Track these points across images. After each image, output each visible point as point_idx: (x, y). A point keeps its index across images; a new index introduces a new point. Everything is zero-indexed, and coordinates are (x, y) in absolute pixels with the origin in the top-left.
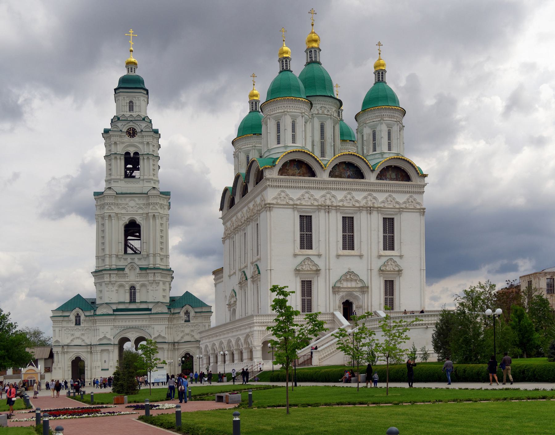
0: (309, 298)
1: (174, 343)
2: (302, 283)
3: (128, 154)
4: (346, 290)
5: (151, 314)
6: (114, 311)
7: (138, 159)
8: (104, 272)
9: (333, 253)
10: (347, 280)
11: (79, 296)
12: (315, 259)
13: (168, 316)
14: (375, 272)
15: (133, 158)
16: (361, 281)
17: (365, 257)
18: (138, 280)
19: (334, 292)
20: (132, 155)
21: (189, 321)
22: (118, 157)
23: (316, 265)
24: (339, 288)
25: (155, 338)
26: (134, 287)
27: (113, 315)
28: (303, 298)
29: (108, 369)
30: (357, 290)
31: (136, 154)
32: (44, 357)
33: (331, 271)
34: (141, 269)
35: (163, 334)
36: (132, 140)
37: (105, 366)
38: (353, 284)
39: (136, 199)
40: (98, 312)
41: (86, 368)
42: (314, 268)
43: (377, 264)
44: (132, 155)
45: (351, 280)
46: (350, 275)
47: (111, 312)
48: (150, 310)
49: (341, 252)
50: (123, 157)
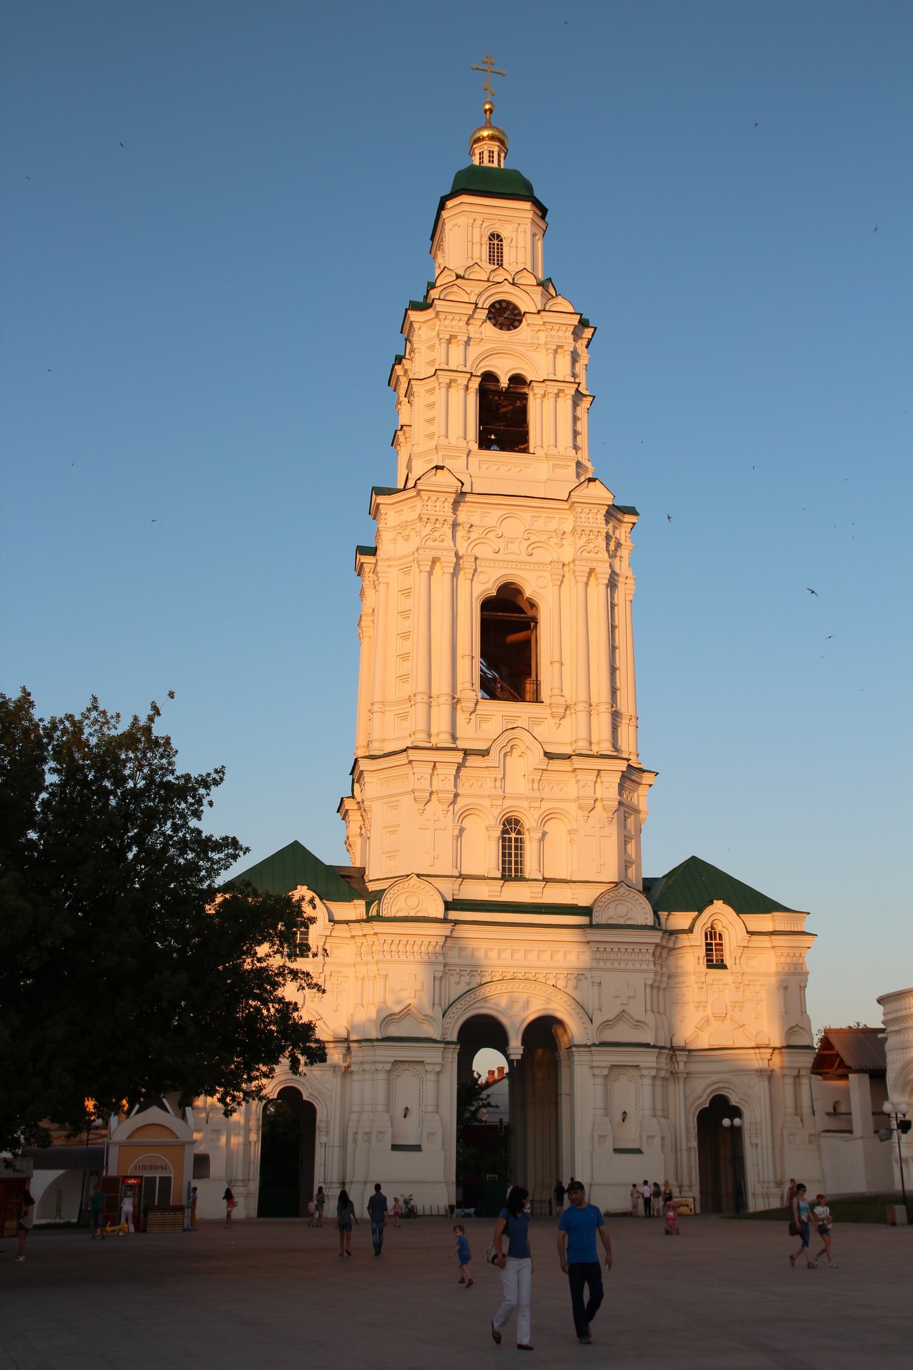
1: (673, 1049)
3: (489, 378)
5: (591, 926)
6: (449, 906)
7: (524, 397)
8: (413, 755)
11: (296, 847)
13: (656, 937)
15: (508, 393)
18: (537, 794)
20: (504, 383)
21: (722, 966)
22: (462, 380)
25: (607, 1024)
26: (517, 822)
27: (445, 920)
29: (417, 1148)
31: (517, 380)
32: (772, 1045)
34: (549, 756)
35: (637, 1009)
36: (505, 335)
37: (409, 1133)
39: (527, 515)
40: (390, 906)
41: (320, 1138)
44: (504, 383)
47: (438, 911)
48: (586, 911)
50: (475, 384)
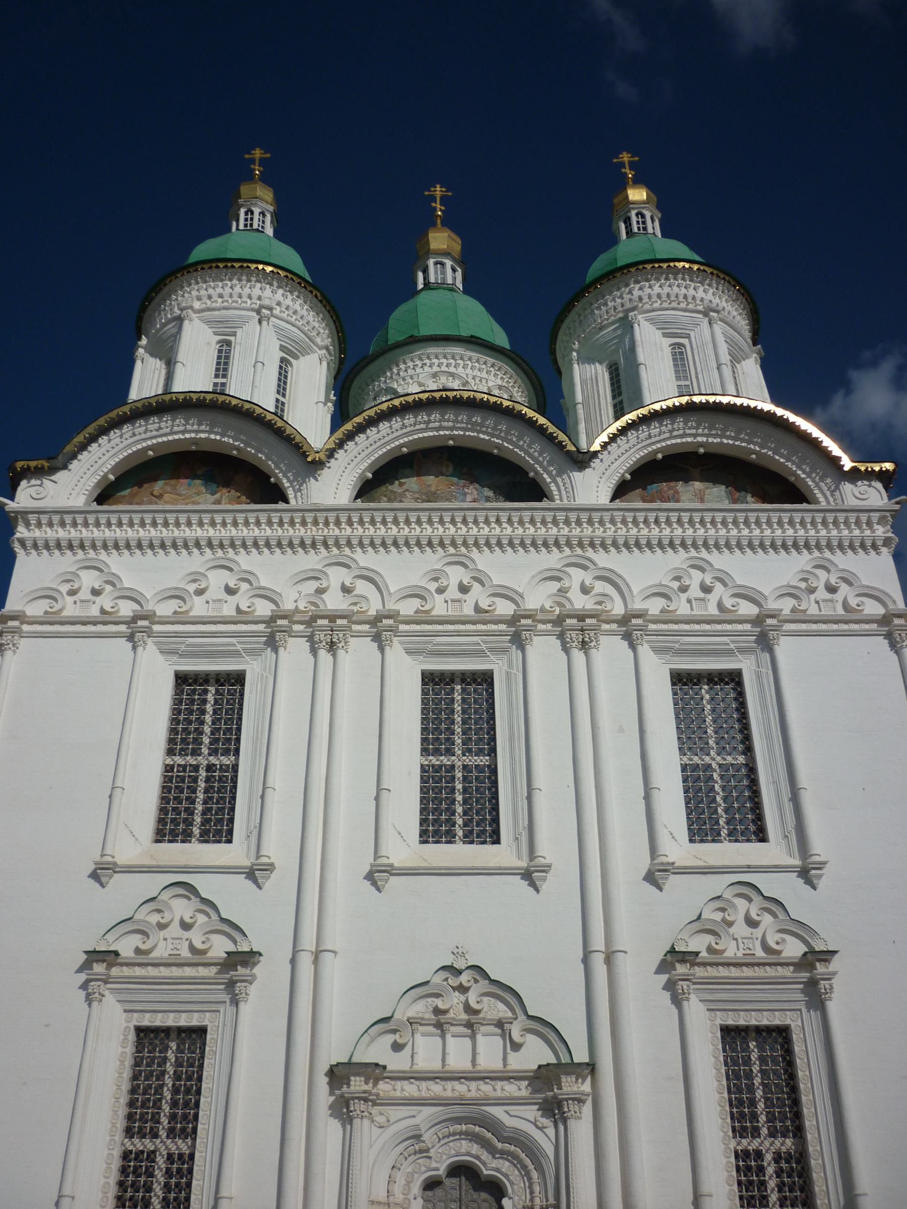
0: (183, 1146)
2: (139, 1046)
4: (436, 1089)
9: (348, 860)
10: (440, 1023)
12: (231, 896)
14: (639, 978)
16: (544, 1028)
17: (561, 882)
19: (343, 1110)
23: (232, 928)
24: (374, 1071)
28: (138, 1144)
30: (511, 1089)
33: (327, 958)
38: (490, 1052)
42: (220, 947)
43: (646, 923)
45: (472, 1024)
46: (468, 993)
49: (403, 842)
